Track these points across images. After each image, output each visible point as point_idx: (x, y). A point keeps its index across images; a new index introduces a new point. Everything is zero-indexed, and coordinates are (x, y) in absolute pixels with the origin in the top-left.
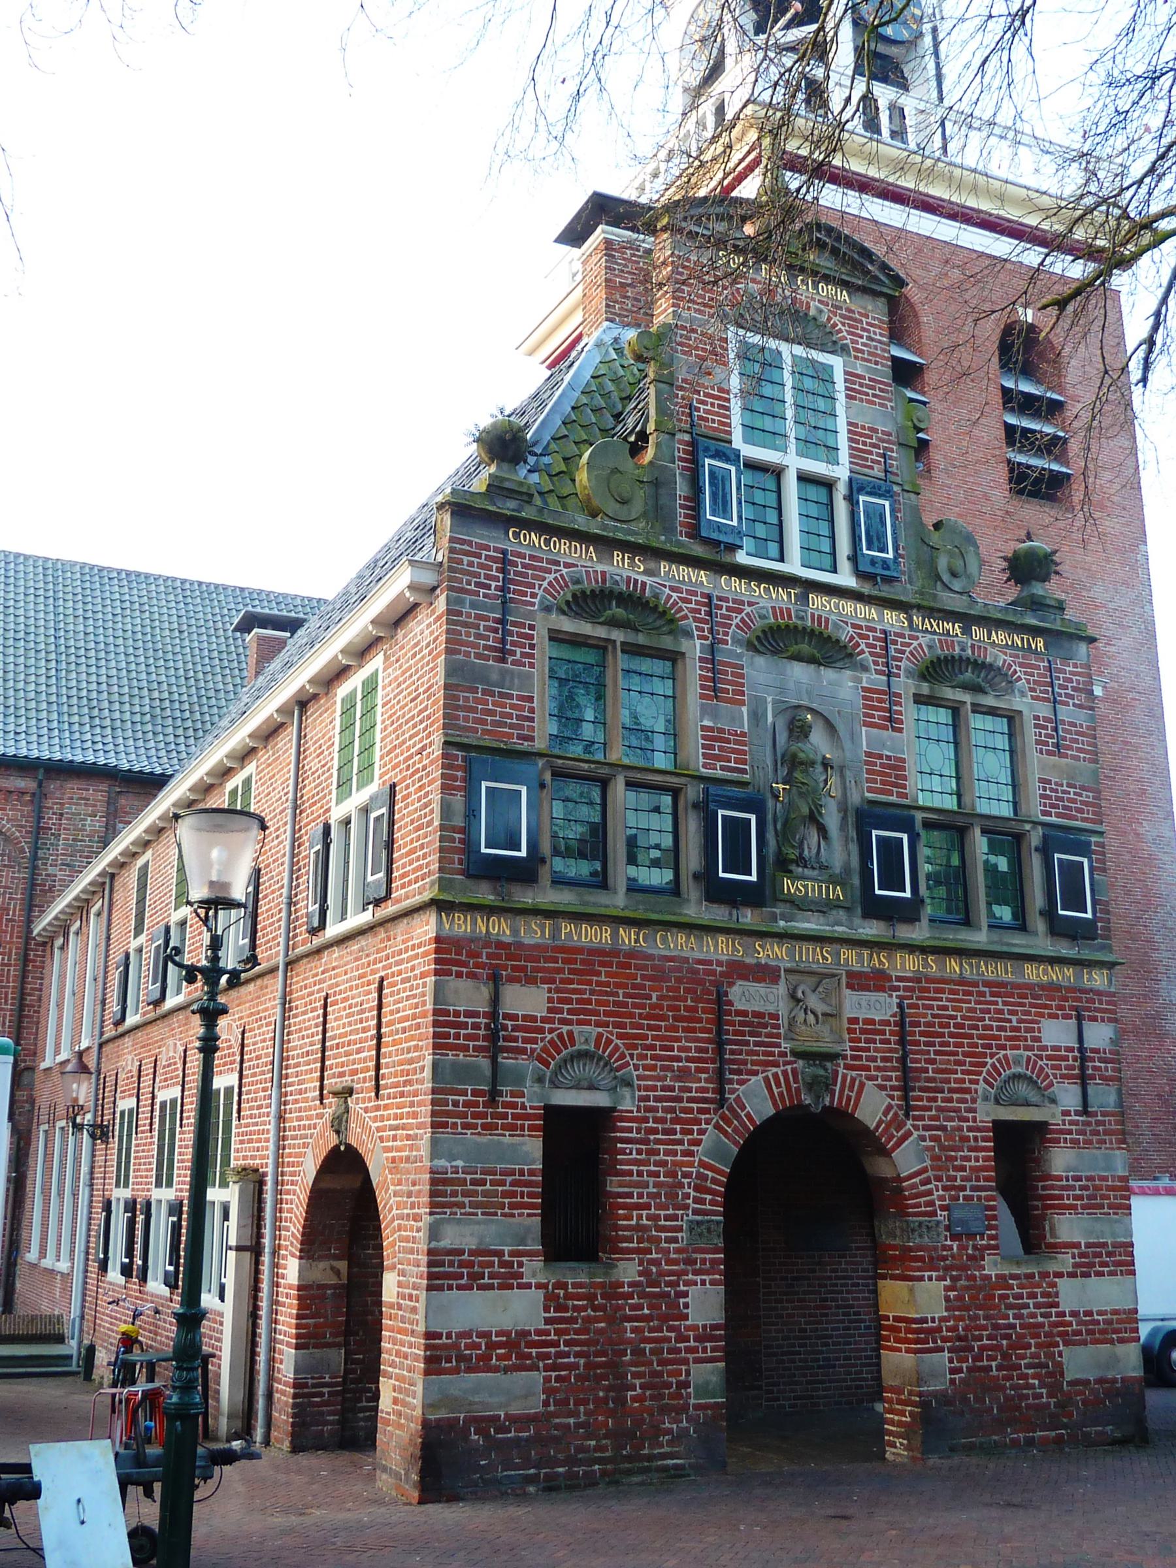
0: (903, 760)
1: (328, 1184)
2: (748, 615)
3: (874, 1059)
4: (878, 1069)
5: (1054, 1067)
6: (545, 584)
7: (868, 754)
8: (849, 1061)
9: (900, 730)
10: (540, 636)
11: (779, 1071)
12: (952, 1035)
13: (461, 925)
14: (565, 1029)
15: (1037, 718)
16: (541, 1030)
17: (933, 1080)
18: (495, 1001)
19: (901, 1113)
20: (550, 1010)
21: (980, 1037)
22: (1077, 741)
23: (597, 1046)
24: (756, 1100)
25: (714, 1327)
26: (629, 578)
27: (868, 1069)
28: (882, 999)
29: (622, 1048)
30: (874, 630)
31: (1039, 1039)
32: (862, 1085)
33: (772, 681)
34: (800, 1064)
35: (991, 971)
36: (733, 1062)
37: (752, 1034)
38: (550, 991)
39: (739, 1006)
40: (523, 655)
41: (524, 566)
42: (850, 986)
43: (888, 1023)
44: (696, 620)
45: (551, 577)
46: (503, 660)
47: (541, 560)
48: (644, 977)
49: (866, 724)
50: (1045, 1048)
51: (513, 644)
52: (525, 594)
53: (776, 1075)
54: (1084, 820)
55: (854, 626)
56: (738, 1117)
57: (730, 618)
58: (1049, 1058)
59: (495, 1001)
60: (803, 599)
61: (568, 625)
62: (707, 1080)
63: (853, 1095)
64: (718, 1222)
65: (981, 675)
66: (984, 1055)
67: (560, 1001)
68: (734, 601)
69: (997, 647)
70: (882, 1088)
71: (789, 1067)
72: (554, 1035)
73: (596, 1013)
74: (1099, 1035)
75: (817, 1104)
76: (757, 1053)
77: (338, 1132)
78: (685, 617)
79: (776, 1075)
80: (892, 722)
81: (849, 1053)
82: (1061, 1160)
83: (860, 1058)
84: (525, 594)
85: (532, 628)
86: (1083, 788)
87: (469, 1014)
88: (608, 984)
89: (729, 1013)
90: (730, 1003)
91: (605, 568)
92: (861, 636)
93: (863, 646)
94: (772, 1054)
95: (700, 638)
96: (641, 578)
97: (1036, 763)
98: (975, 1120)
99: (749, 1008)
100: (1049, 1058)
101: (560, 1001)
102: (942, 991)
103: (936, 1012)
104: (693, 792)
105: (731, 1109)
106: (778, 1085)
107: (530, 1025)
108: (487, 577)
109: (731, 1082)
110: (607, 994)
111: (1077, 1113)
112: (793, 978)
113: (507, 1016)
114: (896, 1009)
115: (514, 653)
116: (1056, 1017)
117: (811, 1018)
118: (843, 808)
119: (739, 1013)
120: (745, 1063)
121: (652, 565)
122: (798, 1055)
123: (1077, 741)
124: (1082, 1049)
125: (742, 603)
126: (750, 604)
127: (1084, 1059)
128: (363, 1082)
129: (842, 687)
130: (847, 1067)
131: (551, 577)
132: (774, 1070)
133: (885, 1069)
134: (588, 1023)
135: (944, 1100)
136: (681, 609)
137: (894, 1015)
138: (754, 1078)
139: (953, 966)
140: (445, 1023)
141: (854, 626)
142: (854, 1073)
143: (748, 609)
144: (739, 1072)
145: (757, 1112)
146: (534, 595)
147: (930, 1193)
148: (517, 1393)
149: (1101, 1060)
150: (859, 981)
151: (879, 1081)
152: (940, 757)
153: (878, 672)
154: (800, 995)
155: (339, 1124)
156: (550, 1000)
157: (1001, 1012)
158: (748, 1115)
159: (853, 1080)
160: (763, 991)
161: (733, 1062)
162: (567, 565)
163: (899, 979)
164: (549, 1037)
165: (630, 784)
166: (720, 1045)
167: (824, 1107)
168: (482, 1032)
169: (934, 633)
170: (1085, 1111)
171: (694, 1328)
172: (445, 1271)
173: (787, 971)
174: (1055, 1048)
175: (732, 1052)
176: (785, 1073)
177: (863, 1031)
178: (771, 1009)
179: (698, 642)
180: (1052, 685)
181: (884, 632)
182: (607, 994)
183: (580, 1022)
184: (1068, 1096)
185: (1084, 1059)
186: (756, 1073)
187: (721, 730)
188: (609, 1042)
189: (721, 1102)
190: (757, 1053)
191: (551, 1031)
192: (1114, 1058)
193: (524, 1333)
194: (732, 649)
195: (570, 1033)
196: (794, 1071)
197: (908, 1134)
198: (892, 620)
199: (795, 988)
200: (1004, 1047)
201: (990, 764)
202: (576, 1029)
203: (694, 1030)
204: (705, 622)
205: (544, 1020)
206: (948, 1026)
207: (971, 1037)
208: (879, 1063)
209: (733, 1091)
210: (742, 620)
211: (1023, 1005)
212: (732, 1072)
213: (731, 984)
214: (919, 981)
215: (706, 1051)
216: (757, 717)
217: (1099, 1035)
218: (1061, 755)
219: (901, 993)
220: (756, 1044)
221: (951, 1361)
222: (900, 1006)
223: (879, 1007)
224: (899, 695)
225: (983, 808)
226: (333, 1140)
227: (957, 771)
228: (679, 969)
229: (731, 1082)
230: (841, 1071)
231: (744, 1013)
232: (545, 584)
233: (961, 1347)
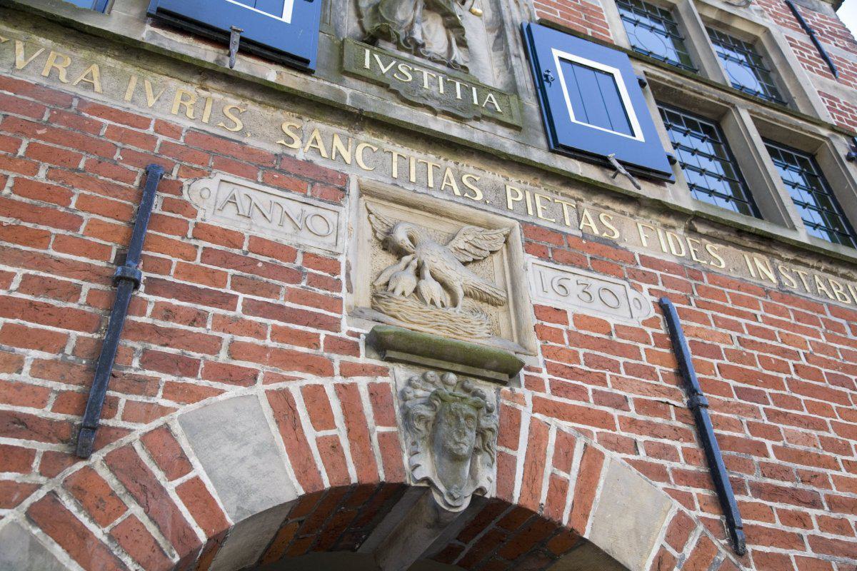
3: (621, 403)
4: (631, 424)
8: (547, 394)
11: (329, 384)
17: (784, 473)
19: (720, 543)
27: (605, 421)
28: (618, 290)
32: (593, 460)
34: (400, 375)
36: (168, 336)
37: (238, 283)
53: (314, 396)
56: (148, 492)
62: (40, 368)
63: (572, 478)
71: (362, 382)
75: (452, 481)
76: (258, 332)
81: (545, 375)
83: (580, 393)
90: (186, 208)
94: (311, 341)
99: (241, 227)
105: (125, 464)
106: (322, 417)
109: (139, 385)
114: (653, 313)
117: (431, 289)
118: (499, 27)
120: (212, 345)
130: (540, 405)
132: (312, 379)
138: (233, 391)
142: (567, 426)
145: (230, 485)
151: (642, 455)
154: (401, 236)
158: (195, 493)
159: (565, 444)
160: (294, 209)
161: (168, 336)
163: (646, 261)
166: (123, 286)
167: (478, 497)
173: (363, 192)
175: (169, 313)
176: (348, 393)
177: (576, 340)
178: (316, 246)
186: (248, 378)
189: (85, 435)
190: (258, 332)
196: (377, 394)
203: (41, 239)
208: (632, 413)
209: (151, 412)
212: (150, 360)
214: (695, 275)
215: (74, 292)
220: (251, 307)
228: (37, 110)
229: (139, 385)
231: (232, 238)
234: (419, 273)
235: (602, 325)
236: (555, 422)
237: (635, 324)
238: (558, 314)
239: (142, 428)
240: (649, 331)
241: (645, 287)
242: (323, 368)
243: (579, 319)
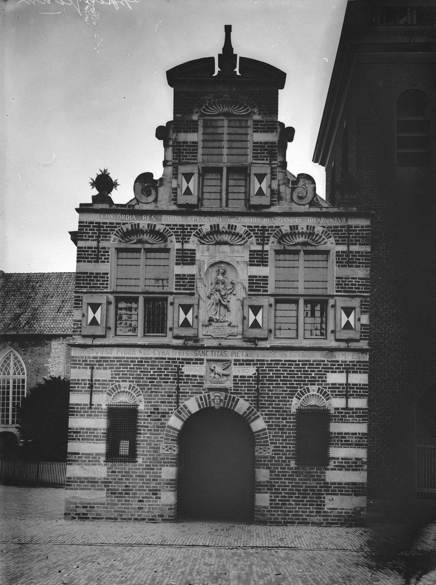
2: (199, 230)
5: (331, 391)
8: (232, 391)
11: (202, 395)
12: (281, 380)
14: (117, 384)
16: (109, 384)
20: (112, 378)
21: (295, 381)
22: (359, 259)
23: (129, 389)
24: (192, 405)
25: (172, 480)
26: (149, 224)
29: (139, 389)
31: (325, 381)
32: (238, 400)
38: (112, 371)
39: (186, 373)
40: (105, 259)
41: (106, 227)
42: (235, 364)
43: (252, 377)
45: (116, 229)
48: (148, 365)
50: (329, 384)
51: (102, 255)
54: (358, 292)
55: (248, 227)
57: (191, 232)
58: (329, 388)
64: (174, 447)
66: (297, 388)
67: (116, 374)
68: (194, 225)
70: (247, 400)
72: (113, 386)
73: (129, 378)
79: (201, 398)
86: (359, 278)
87: (83, 380)
88: (134, 368)
89: (182, 376)
93: (252, 234)
98: (290, 411)
99: (191, 374)
100: (329, 388)
101: (116, 374)
102: (278, 364)
103: (274, 372)
107: (104, 383)
110: (133, 371)
111: (342, 409)
112: (211, 363)
113: (96, 380)
115: (101, 259)
116: (336, 372)
117: (217, 376)
119: (186, 376)
122: (208, 389)
123: (359, 259)
125: (197, 226)
126: (201, 225)
130: (231, 393)
131: (118, 228)
133: (249, 394)
134: (126, 381)
135: (275, 404)
137: (255, 374)
142: (235, 395)
143: (199, 228)
144: (186, 396)
147: (267, 438)
149: (357, 388)
150: (238, 362)
154: (212, 368)
156: (112, 374)
157: (307, 371)
164: (111, 386)
168: (88, 386)
171: (164, 480)
174: (332, 384)
175: (183, 389)
176: (204, 396)
182: (133, 371)
183: (123, 381)
188: (134, 387)
191: (112, 384)
195: (119, 385)
196: (209, 395)
197: (258, 417)
200: (307, 385)
202: (121, 383)
205: (110, 381)
206: (280, 377)
207: (291, 381)
209: (183, 402)
210: (197, 232)
211: (319, 368)
213: (182, 366)
219: (258, 366)
221: (271, 497)
223: (251, 371)
230: (229, 395)
231: (188, 376)
232: (115, 232)
234: (215, 374)
235: (245, 377)
236: (232, 395)
237: (251, 375)
238: (237, 377)
239: (182, 404)
240: (253, 376)
241: (255, 366)
242: (201, 393)
243: (241, 377)
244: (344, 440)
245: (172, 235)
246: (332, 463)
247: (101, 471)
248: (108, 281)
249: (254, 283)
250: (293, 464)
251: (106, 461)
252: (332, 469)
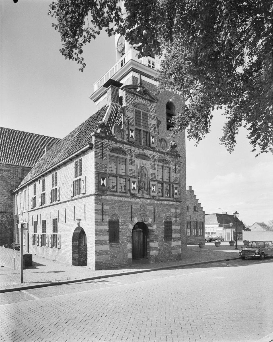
0: (155, 174)
1: (76, 231)
6: (108, 147)
7: (151, 173)
9: (155, 170)
10: (108, 156)
13: (98, 197)
15: (173, 168)
18: (103, 208)
24: (136, 220)
30: (152, 155)
33: (138, 162)
35: (166, 202)
41: (105, 145)
44: (129, 153)
45: (109, 146)
46: (103, 159)
47: (107, 144)
49: (151, 169)
52: (105, 149)
55: (150, 154)
59: (103, 208)
60: (143, 150)
61: (112, 154)
65: (166, 161)
69: (168, 157)
74: (178, 211)
77: (78, 225)
78: (127, 153)
80: (154, 168)
82: (174, 227)
84: (105, 149)
85: (106, 154)
86: (178, 178)
91: (116, 145)
92: (150, 156)
95: (129, 156)
96: (121, 147)
97: (173, 175)
104: (128, 179)
108: (100, 146)
115: (104, 158)
121: (123, 144)
124: (176, 213)
125: (135, 151)
126: (136, 151)
127: (176, 214)
128: (82, 218)
129: (148, 164)
131: (109, 146)
136: (127, 152)
139: (161, 202)
140: (96, 211)
141: (150, 154)
146: (107, 149)
148: (106, 258)
152: (160, 174)
153: (153, 161)
155: (78, 224)
156: (110, 207)
162: (111, 145)
165: (120, 177)
169: (160, 155)
170: (176, 221)
172: (97, 243)
179: (129, 157)
180: (175, 163)
181: (154, 155)
184: (174, 219)
185: (176, 214)
187: (132, 170)
192: (180, 214)
193: (107, 250)
194: (134, 158)
198: (155, 154)
199: (141, 205)
201: (166, 175)
204: (130, 153)
216: (137, 167)
217: (178, 211)
218: (176, 173)
222: (154, 207)
224: (155, 165)
225: (166, 181)
226: (77, 226)
227: (162, 175)
233: (159, 250)
244: (177, 231)
245: (127, 153)
246: (173, 239)
247: (107, 247)
248: (107, 168)
249: (152, 176)
250: (164, 241)
251: (109, 243)
252: (173, 241)
